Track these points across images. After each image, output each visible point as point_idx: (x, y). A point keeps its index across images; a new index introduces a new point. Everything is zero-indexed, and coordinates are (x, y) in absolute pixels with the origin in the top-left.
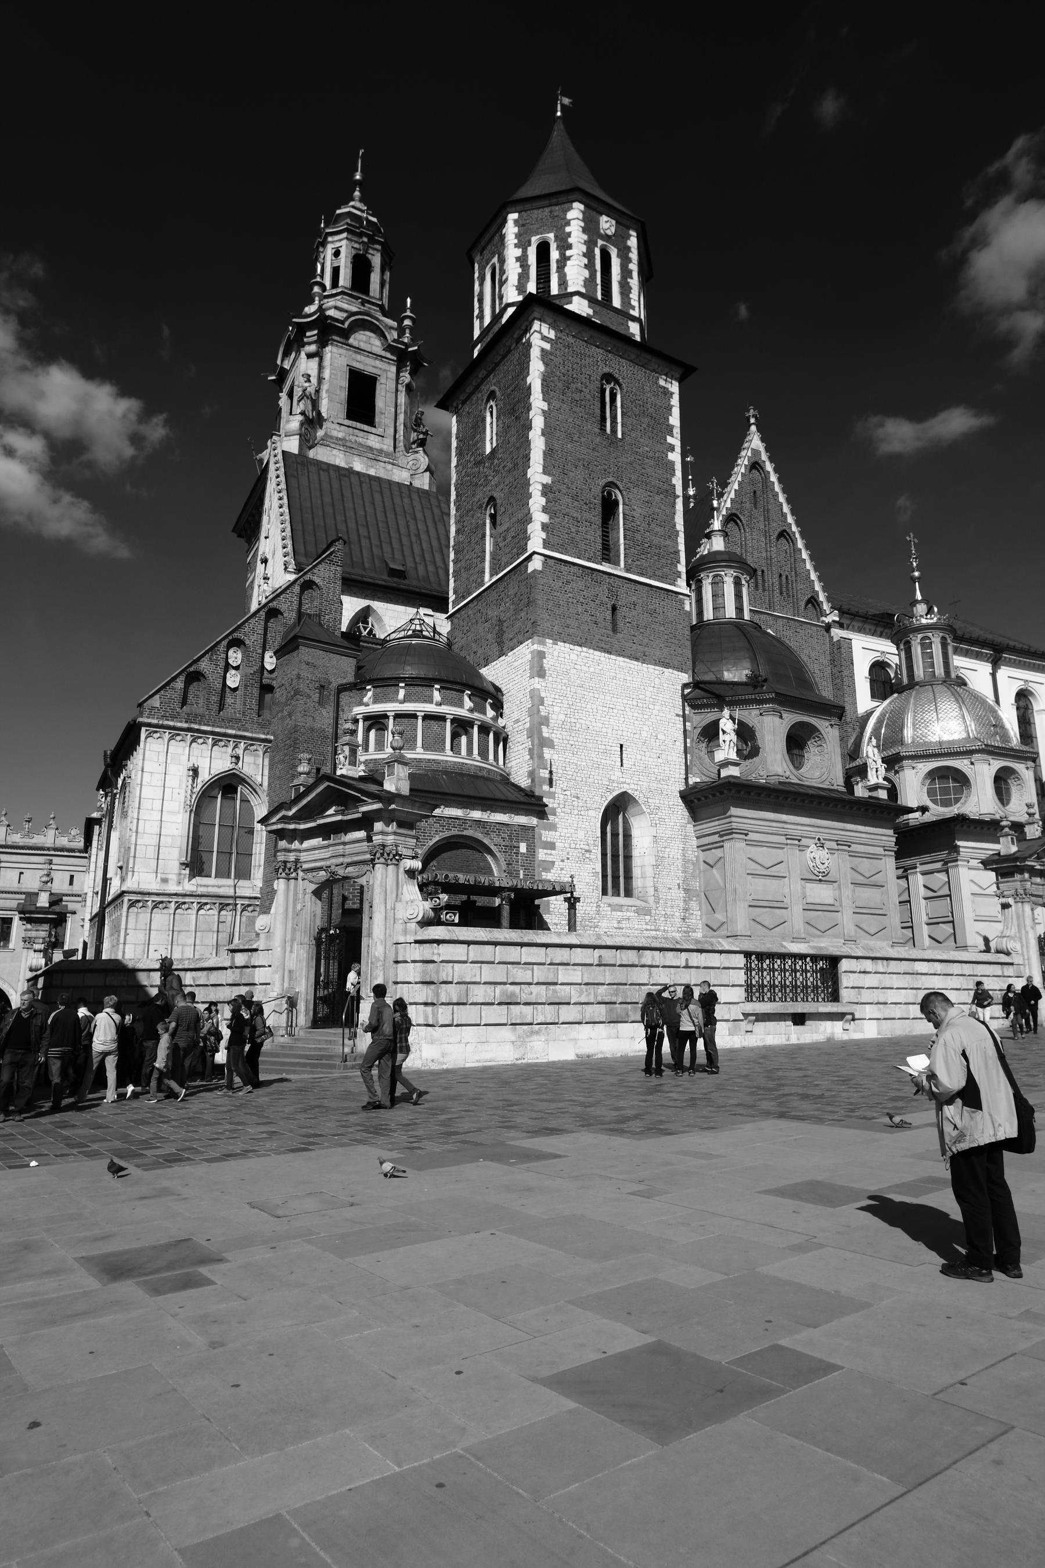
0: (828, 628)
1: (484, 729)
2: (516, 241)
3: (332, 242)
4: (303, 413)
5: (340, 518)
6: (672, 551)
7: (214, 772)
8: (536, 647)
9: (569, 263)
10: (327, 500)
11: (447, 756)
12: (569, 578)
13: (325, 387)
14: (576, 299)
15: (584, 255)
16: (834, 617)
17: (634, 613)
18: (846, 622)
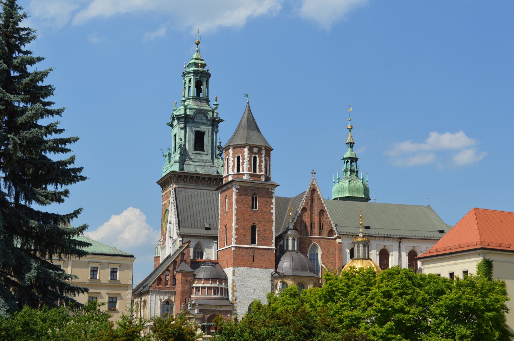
0: (336, 239)
1: (221, 288)
2: (232, 155)
3: (188, 76)
4: (180, 154)
5: (191, 210)
6: (271, 237)
7: (165, 299)
8: (232, 269)
9: (244, 164)
10: (188, 204)
11: (213, 296)
12: (242, 250)
13: (187, 139)
14: (246, 175)
15: (248, 161)
16: (337, 235)
17: (259, 256)
18: (341, 236)
